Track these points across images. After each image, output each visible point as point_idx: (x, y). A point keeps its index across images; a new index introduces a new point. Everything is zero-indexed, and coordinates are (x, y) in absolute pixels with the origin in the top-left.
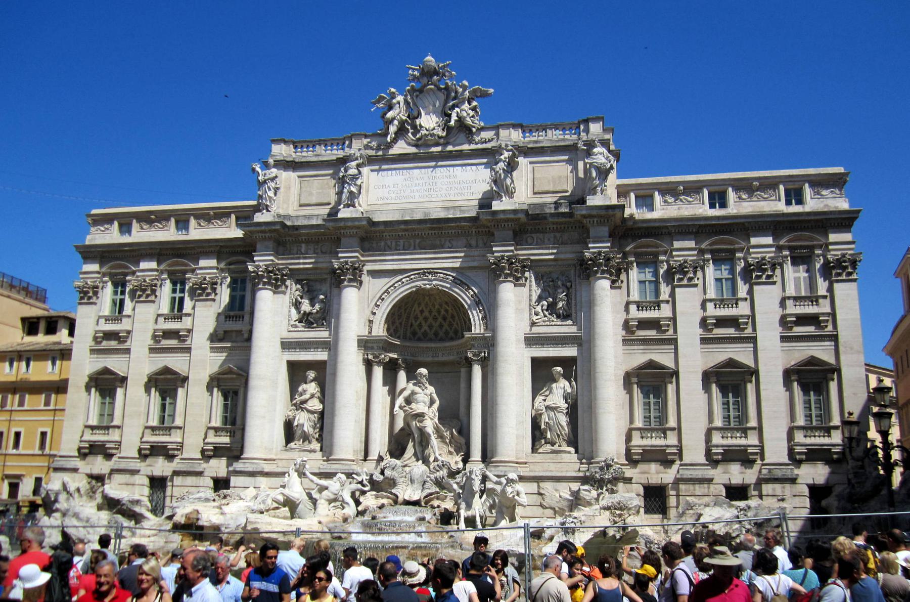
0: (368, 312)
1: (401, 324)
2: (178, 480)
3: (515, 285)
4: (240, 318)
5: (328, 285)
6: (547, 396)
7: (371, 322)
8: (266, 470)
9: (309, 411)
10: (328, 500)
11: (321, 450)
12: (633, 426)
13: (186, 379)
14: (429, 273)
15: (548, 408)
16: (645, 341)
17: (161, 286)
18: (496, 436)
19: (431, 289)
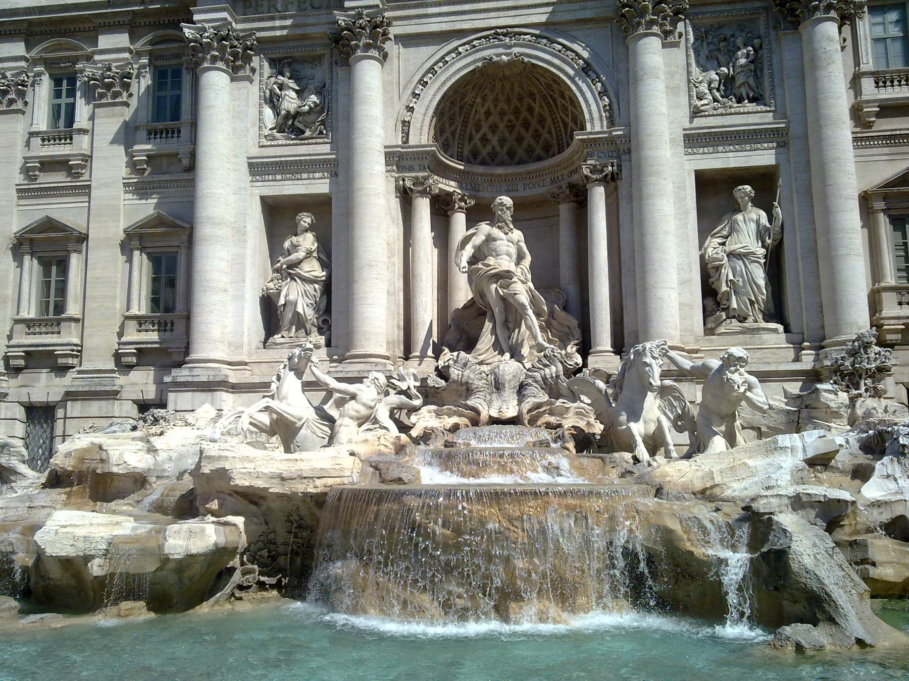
0: (399, 107)
1: (453, 134)
2: (75, 409)
3: (664, 46)
4: (174, 132)
5: (326, 65)
6: (727, 237)
7: (406, 124)
8: (232, 380)
9: (305, 280)
10: (358, 419)
11: (328, 344)
12: (883, 284)
13: (83, 238)
14: (505, 35)
15: (731, 255)
16: (893, 139)
17: (33, 85)
18: (645, 303)
19: (509, 64)
